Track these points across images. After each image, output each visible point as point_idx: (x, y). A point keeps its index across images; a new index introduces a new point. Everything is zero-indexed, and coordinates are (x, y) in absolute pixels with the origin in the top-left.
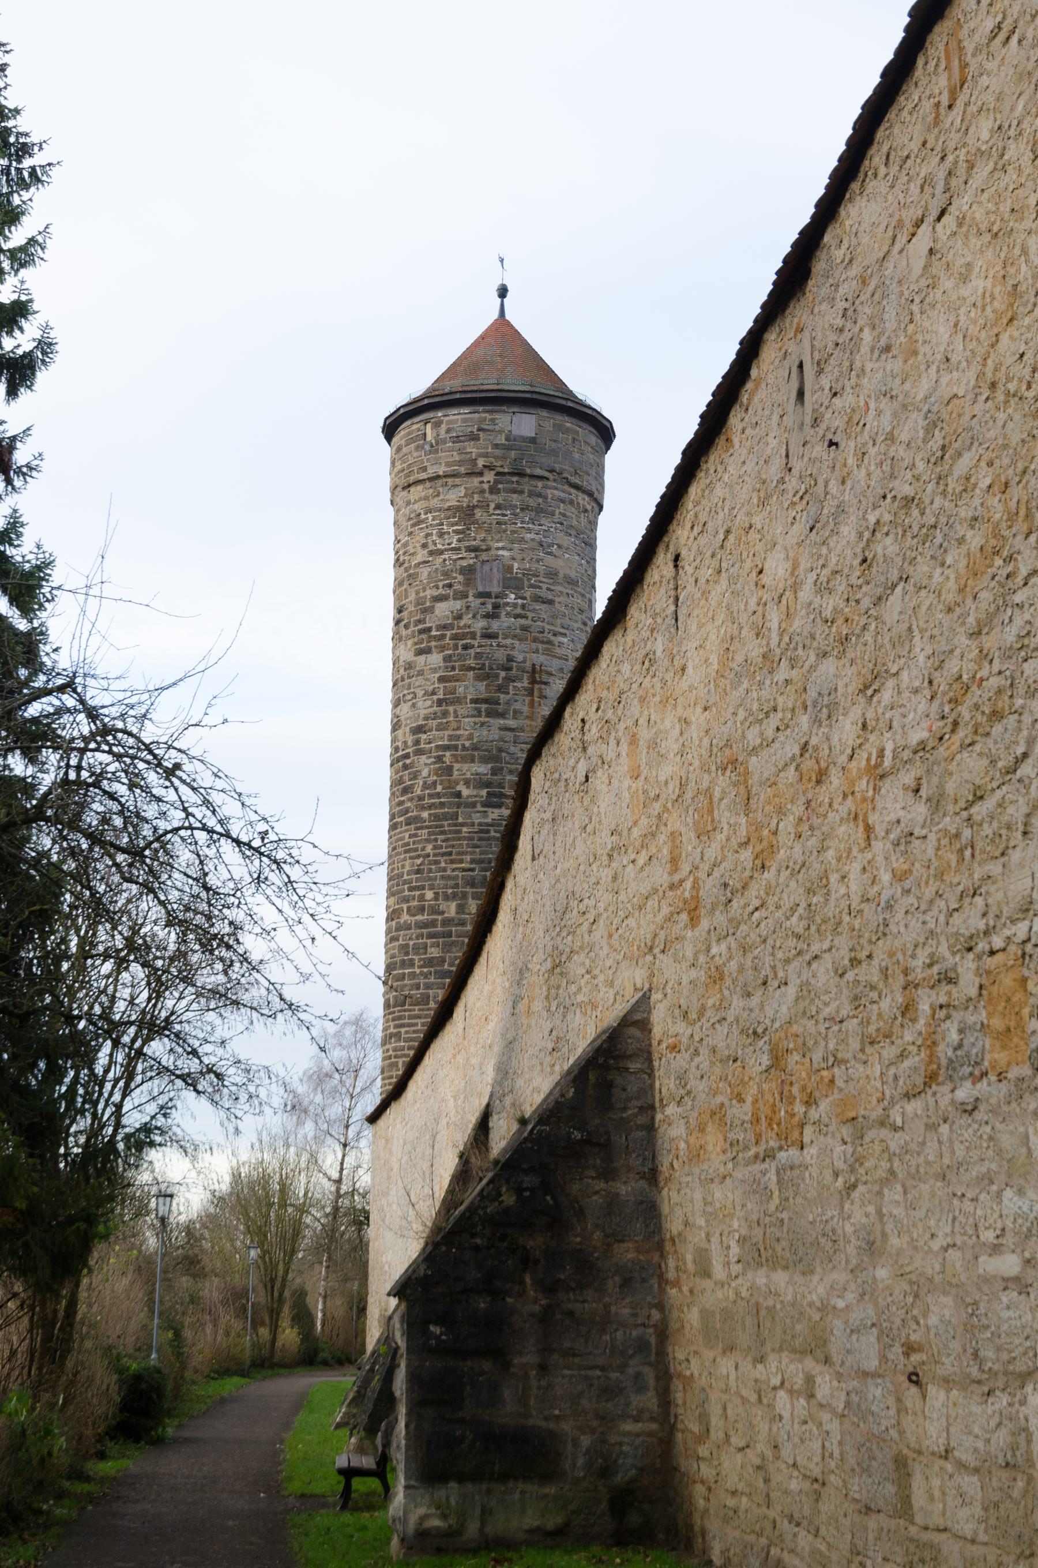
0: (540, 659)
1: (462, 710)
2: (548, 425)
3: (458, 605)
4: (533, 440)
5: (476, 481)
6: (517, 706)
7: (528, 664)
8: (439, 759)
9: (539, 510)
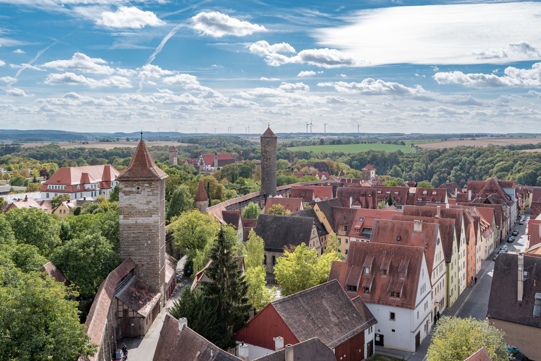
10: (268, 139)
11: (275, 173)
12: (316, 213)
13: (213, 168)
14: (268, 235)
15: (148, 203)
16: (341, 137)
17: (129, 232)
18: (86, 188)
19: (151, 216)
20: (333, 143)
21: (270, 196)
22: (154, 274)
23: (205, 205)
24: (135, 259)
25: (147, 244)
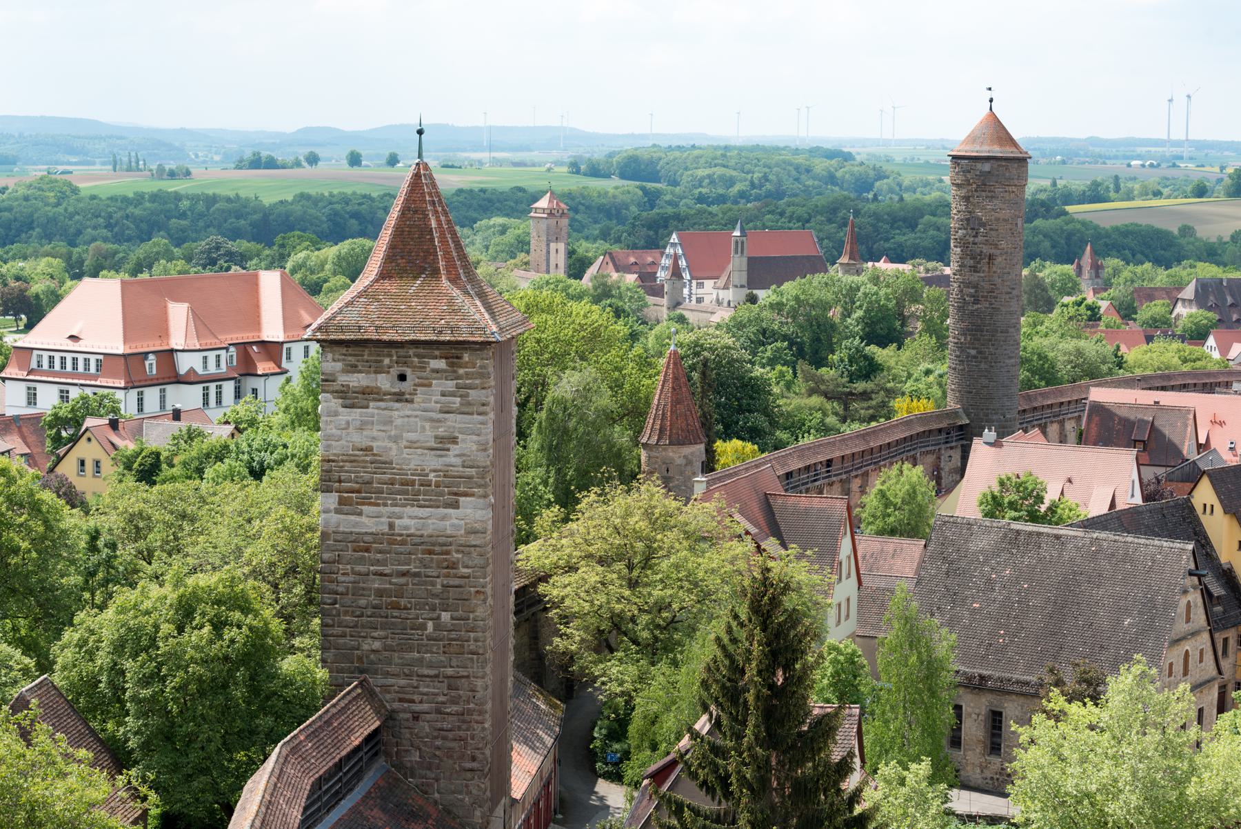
0: (992, 251)
10: (987, 167)
11: (1017, 327)
12: (1206, 520)
14: (974, 612)
15: (446, 442)
17: (359, 568)
18: (183, 369)
19: (455, 505)
22: (462, 757)
23: (689, 463)
24: (386, 689)
25: (436, 628)
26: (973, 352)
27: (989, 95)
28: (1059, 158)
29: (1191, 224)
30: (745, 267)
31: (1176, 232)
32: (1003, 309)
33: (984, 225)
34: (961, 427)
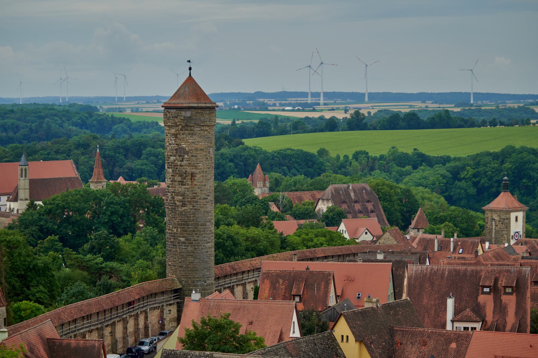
0: (193, 171)
1: (176, 184)
2: (194, 113)
3: (174, 158)
4: (190, 117)
5: (177, 128)
6: (188, 182)
7: (190, 173)
8: (172, 195)
9: (192, 134)
10: (188, 114)
13: (14, 205)
16: (418, 105)
20: (393, 122)
21: (195, 296)
26: (183, 239)
27: (188, 65)
28: (236, 106)
29: (327, 149)
30: (27, 186)
31: (316, 154)
32: (202, 210)
33: (187, 153)
34: (176, 291)
